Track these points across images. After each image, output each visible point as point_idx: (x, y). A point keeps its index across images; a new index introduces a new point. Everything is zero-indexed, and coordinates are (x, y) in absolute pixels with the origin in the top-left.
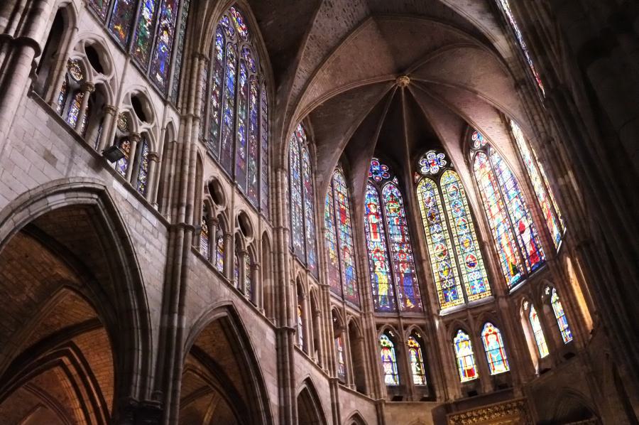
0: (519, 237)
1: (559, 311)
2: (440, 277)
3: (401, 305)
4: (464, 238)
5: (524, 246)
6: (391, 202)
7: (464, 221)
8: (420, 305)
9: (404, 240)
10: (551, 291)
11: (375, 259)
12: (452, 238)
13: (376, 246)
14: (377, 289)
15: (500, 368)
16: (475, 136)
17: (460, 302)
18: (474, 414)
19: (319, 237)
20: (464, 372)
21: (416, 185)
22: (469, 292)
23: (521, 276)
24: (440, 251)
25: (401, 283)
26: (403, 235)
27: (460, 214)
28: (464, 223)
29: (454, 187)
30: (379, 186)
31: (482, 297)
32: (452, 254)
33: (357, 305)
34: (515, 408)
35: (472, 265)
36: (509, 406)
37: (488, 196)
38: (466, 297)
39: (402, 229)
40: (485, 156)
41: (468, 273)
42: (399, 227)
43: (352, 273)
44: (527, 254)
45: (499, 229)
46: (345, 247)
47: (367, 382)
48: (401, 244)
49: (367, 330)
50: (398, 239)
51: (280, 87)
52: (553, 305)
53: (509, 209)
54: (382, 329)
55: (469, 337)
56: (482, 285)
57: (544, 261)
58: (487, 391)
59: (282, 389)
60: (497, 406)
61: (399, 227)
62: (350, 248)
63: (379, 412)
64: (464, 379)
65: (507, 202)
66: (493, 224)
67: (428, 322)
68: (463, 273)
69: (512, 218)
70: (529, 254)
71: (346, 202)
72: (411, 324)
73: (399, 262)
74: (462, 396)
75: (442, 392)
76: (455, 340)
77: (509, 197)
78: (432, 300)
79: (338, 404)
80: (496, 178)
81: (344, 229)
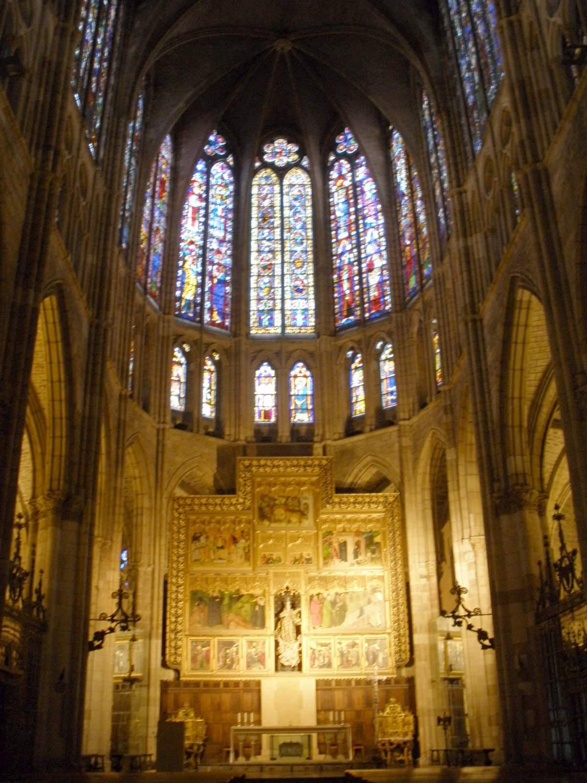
3: (207, 318)
5: (368, 288)
6: (220, 185)
7: (302, 236)
8: (227, 323)
9: (225, 237)
10: (383, 347)
11: (187, 252)
12: (283, 251)
14: (182, 289)
15: (303, 418)
16: (341, 137)
17: (276, 330)
18: (269, 463)
19: (136, 210)
21: (255, 172)
25: (211, 289)
26: (226, 230)
27: (299, 225)
28: (300, 238)
29: (299, 191)
30: (211, 161)
32: (278, 271)
34: (315, 466)
35: (299, 291)
36: (310, 462)
37: (338, 214)
38: (283, 326)
39: (225, 223)
40: (348, 166)
41: (292, 299)
42: (223, 220)
43: (159, 263)
44: (369, 297)
45: (343, 258)
46: (158, 229)
47: (152, 400)
48: (221, 241)
49: (163, 337)
50: (220, 234)
51: (141, 7)
52: (381, 364)
54: (180, 340)
55: (276, 373)
56: (305, 318)
57: (387, 313)
58: (284, 440)
59: (88, 395)
61: (223, 220)
62: (162, 232)
63: (161, 438)
64: (258, 419)
65: (361, 230)
66: (337, 249)
67: (233, 345)
68: (288, 295)
69: (363, 251)
71: (169, 171)
72: (213, 343)
73: (212, 263)
74: (254, 440)
75: (233, 430)
76: (258, 373)
77: (365, 224)
78: (243, 320)
79: (124, 421)
80: (355, 196)
81: (161, 205)
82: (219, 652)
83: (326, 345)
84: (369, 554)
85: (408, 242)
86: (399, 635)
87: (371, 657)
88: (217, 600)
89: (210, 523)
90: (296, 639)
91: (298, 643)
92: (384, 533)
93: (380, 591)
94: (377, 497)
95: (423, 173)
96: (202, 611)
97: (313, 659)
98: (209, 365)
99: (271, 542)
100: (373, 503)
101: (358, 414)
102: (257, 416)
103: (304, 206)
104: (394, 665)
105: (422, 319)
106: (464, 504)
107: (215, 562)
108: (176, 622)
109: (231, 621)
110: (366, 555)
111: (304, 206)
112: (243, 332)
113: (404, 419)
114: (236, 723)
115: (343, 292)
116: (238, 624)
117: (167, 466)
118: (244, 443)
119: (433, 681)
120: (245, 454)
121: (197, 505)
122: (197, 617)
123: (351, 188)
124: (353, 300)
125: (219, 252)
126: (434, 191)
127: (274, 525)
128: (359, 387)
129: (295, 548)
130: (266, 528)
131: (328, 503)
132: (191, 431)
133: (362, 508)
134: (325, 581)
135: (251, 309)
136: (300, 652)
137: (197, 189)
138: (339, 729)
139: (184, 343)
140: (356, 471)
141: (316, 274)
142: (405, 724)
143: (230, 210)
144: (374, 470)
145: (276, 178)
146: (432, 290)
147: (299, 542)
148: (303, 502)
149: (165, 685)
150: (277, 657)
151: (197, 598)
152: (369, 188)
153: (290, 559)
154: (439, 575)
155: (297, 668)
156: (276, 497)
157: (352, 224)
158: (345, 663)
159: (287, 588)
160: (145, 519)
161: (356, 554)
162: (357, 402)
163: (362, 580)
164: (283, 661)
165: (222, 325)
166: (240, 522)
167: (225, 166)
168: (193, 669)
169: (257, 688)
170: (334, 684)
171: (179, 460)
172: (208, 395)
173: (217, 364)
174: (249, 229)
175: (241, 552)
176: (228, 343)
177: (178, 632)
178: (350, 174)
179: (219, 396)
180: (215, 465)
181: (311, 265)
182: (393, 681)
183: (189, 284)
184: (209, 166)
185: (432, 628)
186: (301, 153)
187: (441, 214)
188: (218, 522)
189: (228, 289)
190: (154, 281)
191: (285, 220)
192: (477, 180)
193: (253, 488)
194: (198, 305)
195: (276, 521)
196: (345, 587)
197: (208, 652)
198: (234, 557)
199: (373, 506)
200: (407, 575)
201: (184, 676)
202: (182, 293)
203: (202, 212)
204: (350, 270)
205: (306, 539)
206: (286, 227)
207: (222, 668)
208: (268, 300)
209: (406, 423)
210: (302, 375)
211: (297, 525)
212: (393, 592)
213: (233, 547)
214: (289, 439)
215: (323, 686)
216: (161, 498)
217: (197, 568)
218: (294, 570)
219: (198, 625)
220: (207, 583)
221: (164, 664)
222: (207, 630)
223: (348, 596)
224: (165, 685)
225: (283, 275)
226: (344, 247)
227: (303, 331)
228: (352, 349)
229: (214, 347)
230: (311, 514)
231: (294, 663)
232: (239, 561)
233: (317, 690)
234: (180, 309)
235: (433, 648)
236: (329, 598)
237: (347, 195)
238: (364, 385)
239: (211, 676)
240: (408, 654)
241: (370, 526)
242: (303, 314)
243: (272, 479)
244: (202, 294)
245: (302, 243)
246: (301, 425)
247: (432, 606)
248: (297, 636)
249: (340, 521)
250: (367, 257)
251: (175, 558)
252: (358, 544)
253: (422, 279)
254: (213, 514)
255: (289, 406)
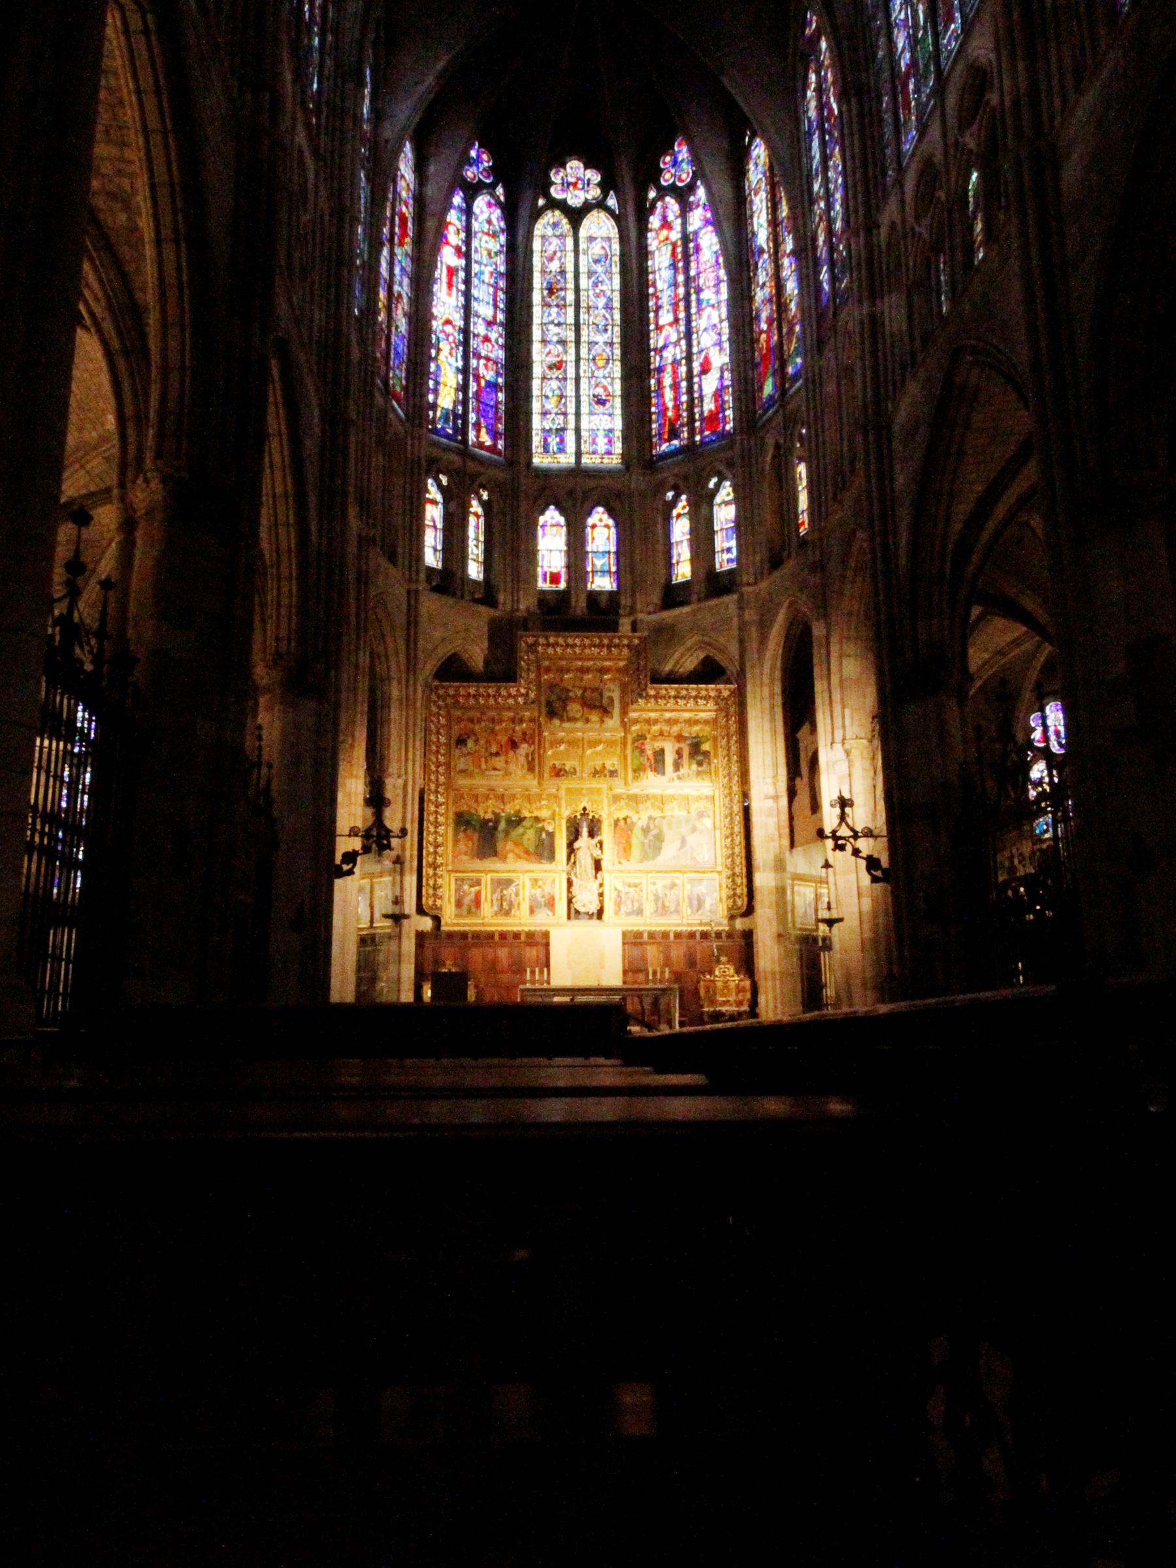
0: (696, 380)
1: (723, 520)
2: (543, 406)
3: (472, 435)
4: (597, 349)
5: (701, 398)
7: (607, 319)
8: (500, 444)
9: (495, 317)
11: (442, 336)
13: (447, 311)
14: (436, 392)
15: (603, 583)
16: (668, 159)
17: (567, 460)
18: (561, 641)
20: (545, 575)
21: (537, 214)
22: (584, 448)
23: (681, 446)
24: (552, 359)
25: (477, 395)
26: (495, 306)
27: (601, 302)
28: (604, 322)
29: (603, 248)
30: (472, 191)
31: (605, 461)
33: (403, 410)
34: (623, 646)
35: (601, 402)
36: (616, 641)
37: (660, 285)
38: (579, 454)
39: (495, 295)
41: (591, 413)
42: (491, 290)
43: (403, 348)
44: (702, 413)
45: (665, 354)
47: (400, 550)
48: (490, 324)
49: (413, 461)
52: (715, 508)
53: (694, 324)
55: (567, 520)
56: (610, 442)
58: (579, 612)
60: (599, 638)
64: (543, 585)
65: (693, 310)
66: (656, 341)
68: (584, 409)
69: (695, 343)
70: (706, 414)
72: (481, 474)
73: (478, 357)
76: (542, 519)
77: (699, 301)
79: (367, 572)
82: (493, 892)
83: (638, 482)
84: (694, 767)
85: (764, 326)
86: (734, 874)
87: (695, 903)
88: (491, 824)
89: (479, 721)
90: (596, 878)
91: (598, 882)
92: (715, 739)
93: (709, 817)
94: (707, 690)
95: (799, 211)
96: (470, 838)
97: (618, 904)
98: (475, 507)
99: (562, 747)
100: (701, 698)
101: (680, 579)
102: (540, 579)
103: (608, 272)
104: (726, 913)
105: (782, 441)
106: (837, 697)
107: (487, 773)
108: (436, 853)
109: (512, 851)
110: (690, 768)
111: (608, 272)
112: (523, 460)
113: (749, 584)
114: (524, 982)
115: (664, 404)
116: (519, 857)
117: (421, 643)
118: (525, 614)
119: (780, 936)
120: (526, 629)
121: (463, 696)
122: (462, 846)
123: (679, 243)
124: (678, 416)
125: (486, 339)
126: (814, 239)
127: (567, 725)
128: (682, 541)
129: (596, 757)
130: (557, 730)
131: (640, 696)
132: (454, 595)
133: (685, 704)
134: (635, 800)
135: (534, 426)
136: (601, 895)
137: (454, 237)
138: (663, 990)
139: (439, 471)
140: (677, 655)
141: (625, 378)
142: (739, 990)
143: (501, 274)
144: (702, 656)
145: (568, 226)
146: (803, 393)
147: (600, 748)
148: (606, 694)
149: (420, 936)
150: (570, 902)
151: (463, 821)
152: (709, 242)
153: (588, 770)
154: (792, 793)
155: (595, 916)
156: (570, 688)
157: (679, 300)
158: (660, 911)
159: (585, 809)
160: (394, 714)
161: (677, 766)
162: (678, 563)
163: (686, 799)
164: (578, 905)
165: (493, 449)
166: (521, 721)
167: (493, 201)
168: (456, 916)
169: (544, 941)
170: (645, 936)
171: (438, 634)
172: (475, 549)
173: (485, 505)
174: (530, 306)
175: (522, 760)
176: (502, 476)
177: (439, 866)
178: (679, 221)
179: (488, 552)
180: (486, 644)
181: (618, 364)
182: (724, 935)
183: (446, 385)
184: (469, 200)
185: (780, 865)
186: (605, 186)
187: (824, 276)
188: (492, 720)
189: (501, 396)
190: (398, 377)
191: (582, 293)
192: (902, 202)
193: (539, 676)
194: (459, 417)
195: (569, 720)
196: (662, 811)
197: (478, 894)
198: (512, 767)
199: (701, 702)
200: (745, 795)
201: (447, 925)
202: (436, 398)
203: (462, 275)
204: (675, 372)
205: (610, 743)
206: (583, 304)
207: (496, 914)
208: (557, 414)
209: (750, 589)
210: (603, 524)
211: (598, 726)
212: (726, 817)
213: (511, 753)
214: (585, 611)
215: (632, 940)
216: (415, 684)
217: (463, 782)
218: (594, 784)
219: (465, 858)
220: (477, 801)
221: (421, 911)
222: (478, 864)
223: (665, 822)
224: (420, 936)
225: (577, 380)
226: (667, 338)
227: (605, 461)
228: (675, 488)
229: (483, 479)
230: (616, 711)
231: (593, 908)
232: (519, 773)
233: (624, 944)
234: (434, 421)
235: (781, 891)
236: (640, 824)
237: (674, 254)
238: (691, 541)
239: (483, 924)
240: (746, 899)
241: (696, 728)
242: (606, 436)
243: (564, 663)
244: (465, 403)
245: (606, 330)
246: (600, 593)
247: (780, 835)
248: (596, 873)
249: (656, 721)
250: (700, 352)
251: (433, 768)
252: (679, 753)
253: (783, 384)
254: (483, 710)
255: (585, 567)
